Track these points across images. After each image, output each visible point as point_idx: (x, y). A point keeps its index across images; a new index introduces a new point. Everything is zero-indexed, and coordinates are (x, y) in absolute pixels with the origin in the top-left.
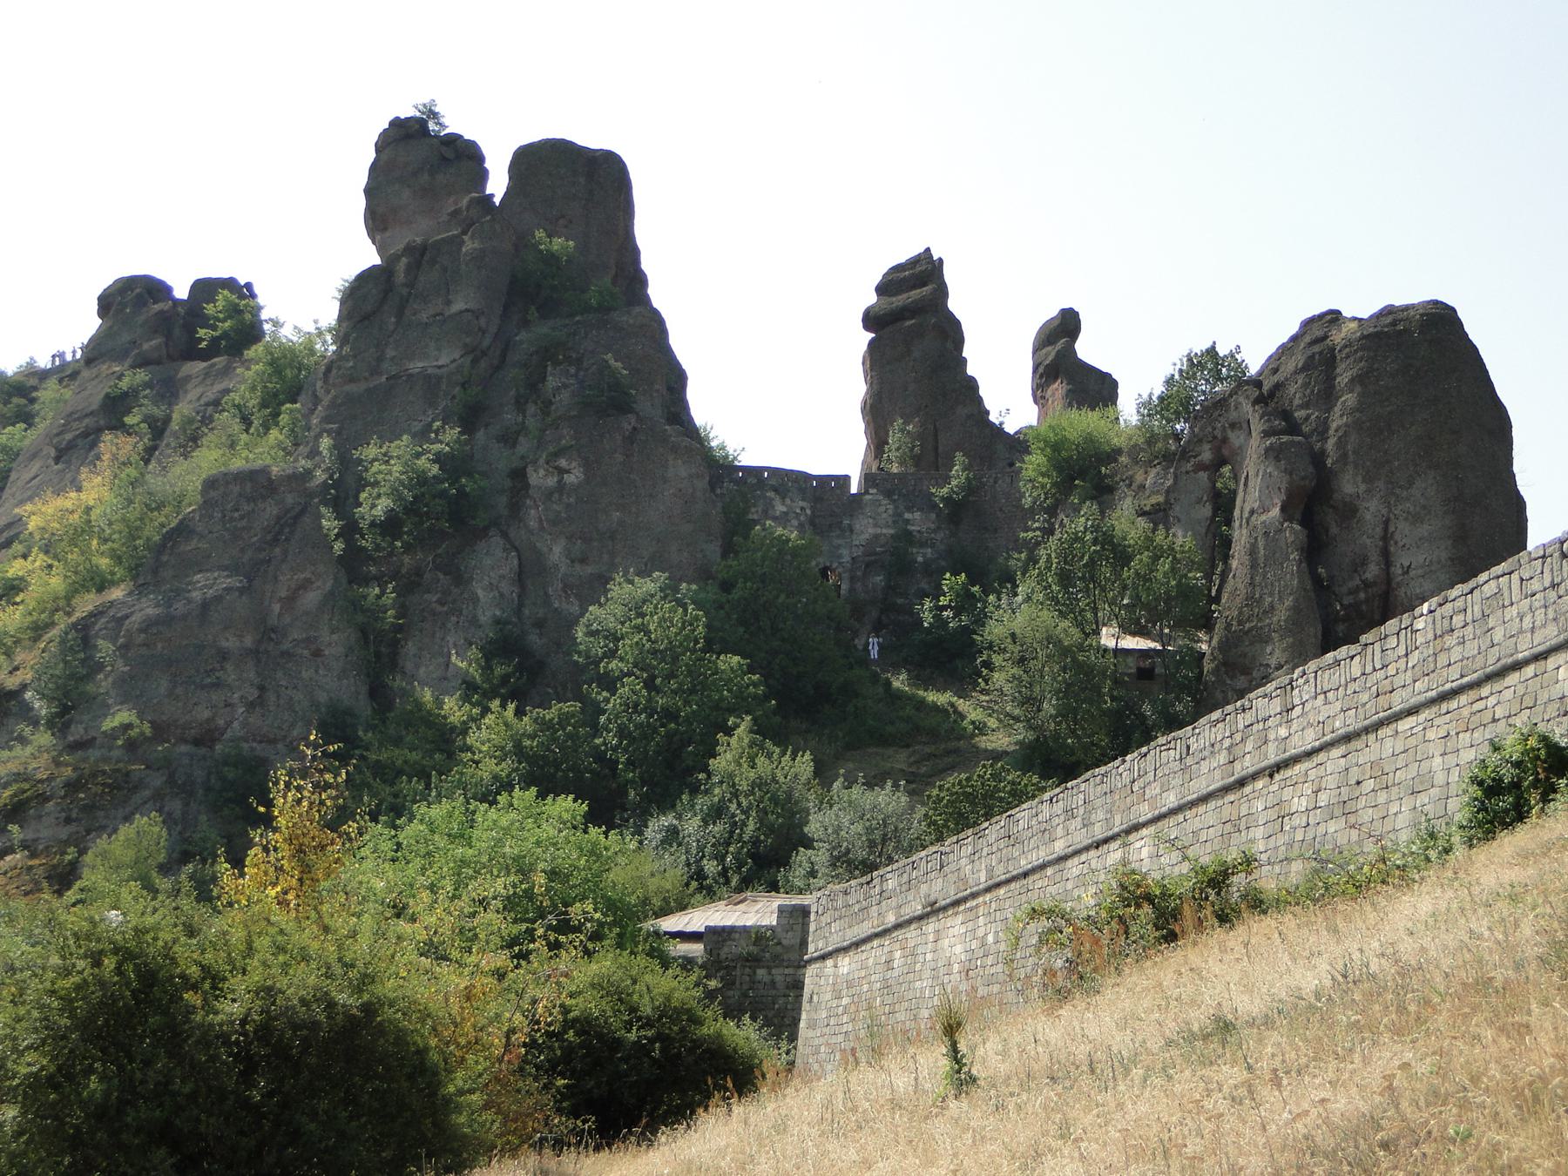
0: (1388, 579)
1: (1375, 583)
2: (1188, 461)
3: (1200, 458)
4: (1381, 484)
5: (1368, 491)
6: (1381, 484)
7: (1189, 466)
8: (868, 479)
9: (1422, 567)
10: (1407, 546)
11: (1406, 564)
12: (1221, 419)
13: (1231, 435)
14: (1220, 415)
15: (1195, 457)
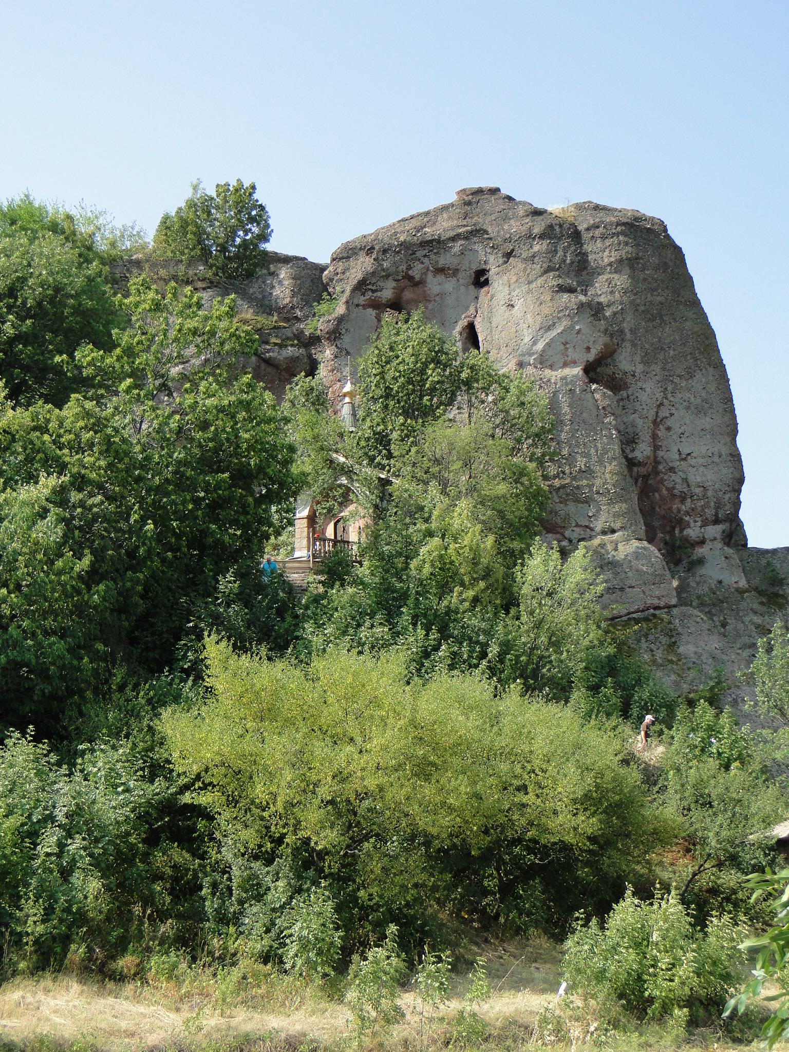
0: (657, 462)
1: (639, 464)
2: (363, 294)
3: (379, 294)
4: (657, 368)
5: (646, 373)
6: (657, 368)
7: (362, 300)
8: (265, 253)
9: (703, 457)
10: (686, 434)
11: (685, 451)
12: (426, 260)
13: (430, 277)
14: (425, 256)
15: (373, 291)
